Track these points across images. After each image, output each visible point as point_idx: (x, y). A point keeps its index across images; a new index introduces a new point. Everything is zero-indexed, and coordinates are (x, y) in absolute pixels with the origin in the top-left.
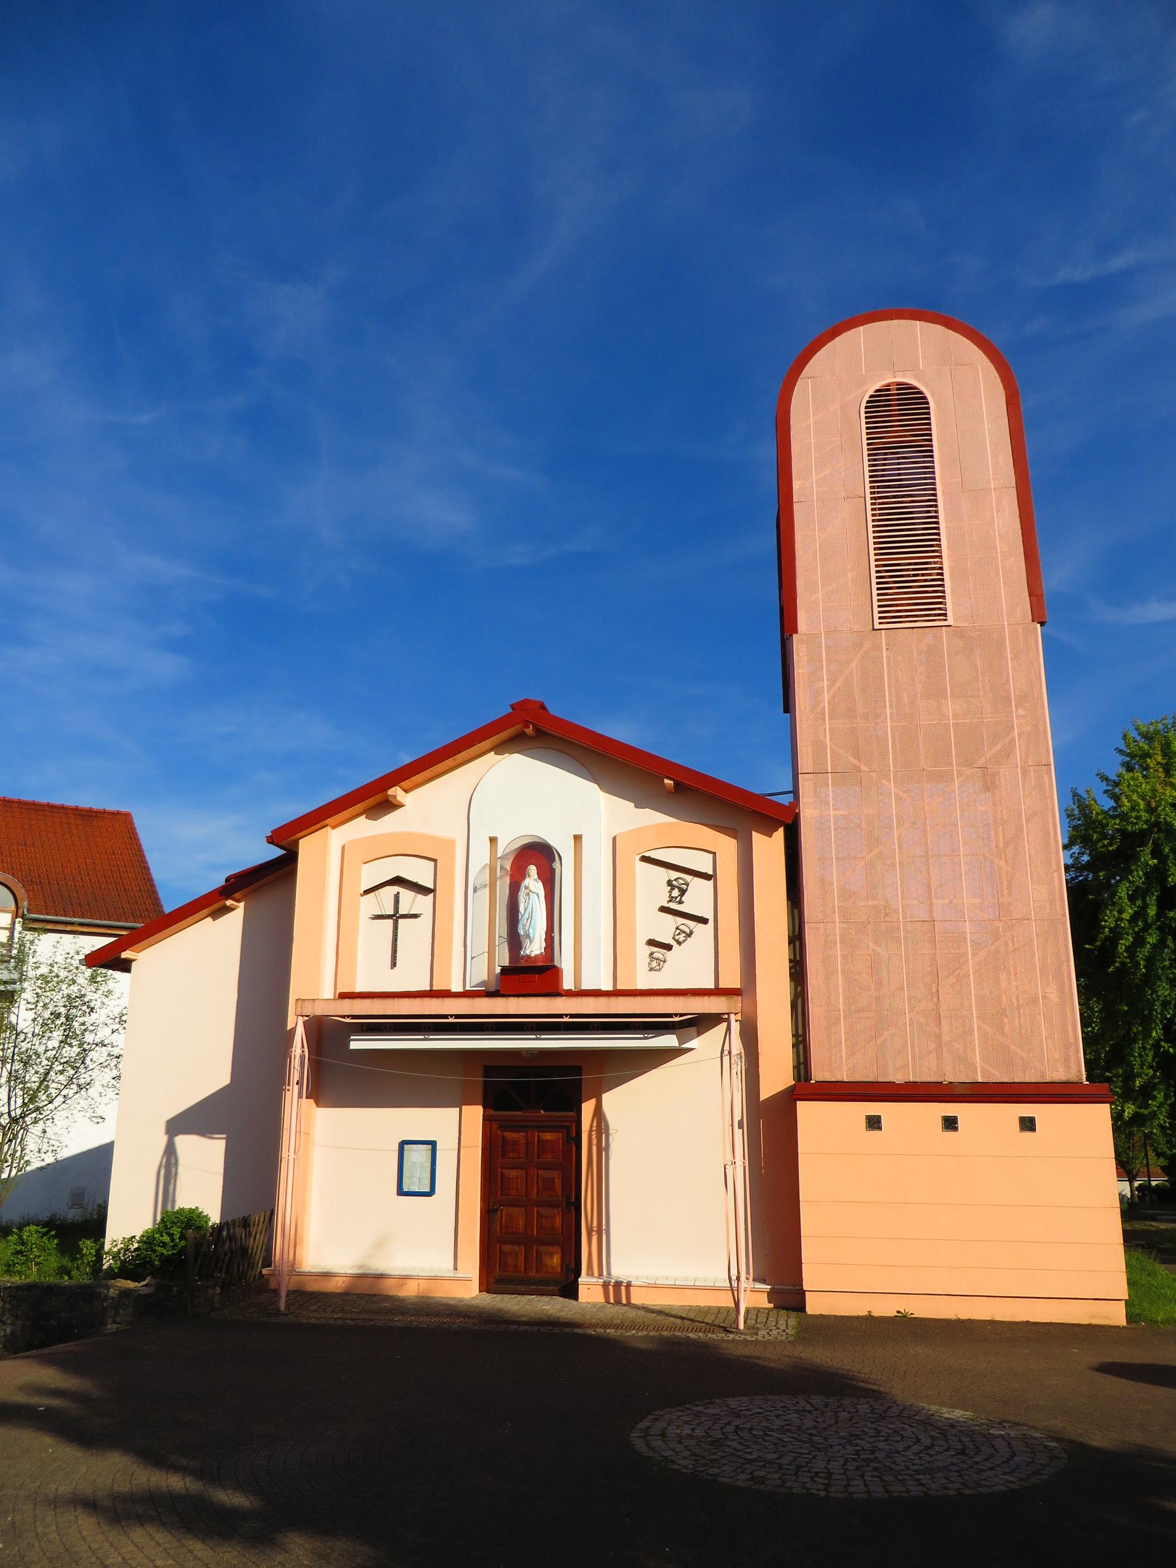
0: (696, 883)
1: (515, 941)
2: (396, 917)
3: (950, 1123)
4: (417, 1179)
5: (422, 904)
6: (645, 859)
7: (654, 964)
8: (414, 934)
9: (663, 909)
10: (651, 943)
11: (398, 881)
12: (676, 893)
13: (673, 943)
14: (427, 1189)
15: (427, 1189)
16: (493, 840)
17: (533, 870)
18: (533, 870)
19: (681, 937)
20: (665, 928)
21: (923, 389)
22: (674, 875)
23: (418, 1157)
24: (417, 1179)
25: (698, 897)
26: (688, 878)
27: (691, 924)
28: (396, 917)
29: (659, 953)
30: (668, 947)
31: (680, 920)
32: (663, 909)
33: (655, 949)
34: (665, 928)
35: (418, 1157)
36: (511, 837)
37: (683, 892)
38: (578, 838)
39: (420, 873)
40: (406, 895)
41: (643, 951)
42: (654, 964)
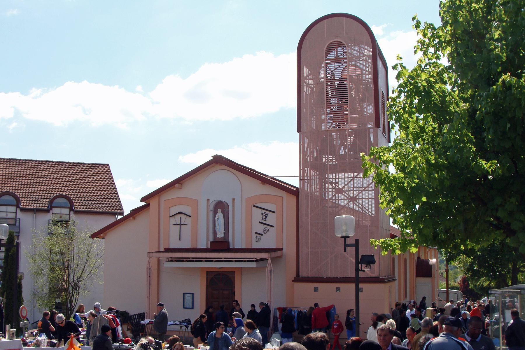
0: (270, 214)
1: (215, 233)
2: (180, 224)
3: (316, 289)
4: (189, 303)
5: (188, 220)
6: (254, 206)
7: (257, 240)
8: (186, 230)
9: (260, 222)
10: (256, 233)
11: (180, 213)
12: (264, 217)
13: (263, 233)
14: (191, 307)
15: (191, 307)
16: (208, 200)
17: (219, 210)
18: (219, 210)
19: (266, 232)
20: (260, 228)
21: (342, 41)
22: (264, 211)
23: (189, 298)
24: (189, 303)
25: (271, 219)
26: (268, 212)
27: (269, 227)
28: (180, 224)
29: (259, 236)
30: (262, 235)
31: (265, 226)
32: (260, 222)
33: (258, 235)
34: (260, 228)
35: (189, 298)
36: (214, 198)
37: (266, 217)
38: (234, 199)
39: (187, 210)
40: (183, 217)
41: (254, 235)
42: (257, 240)
